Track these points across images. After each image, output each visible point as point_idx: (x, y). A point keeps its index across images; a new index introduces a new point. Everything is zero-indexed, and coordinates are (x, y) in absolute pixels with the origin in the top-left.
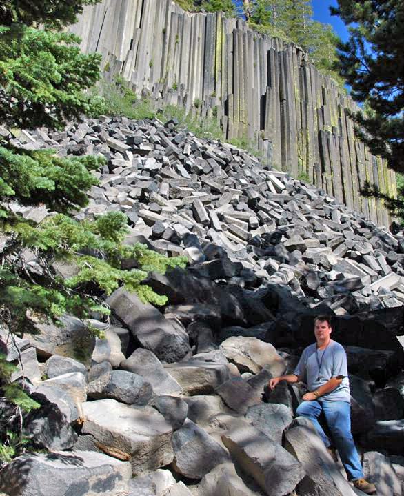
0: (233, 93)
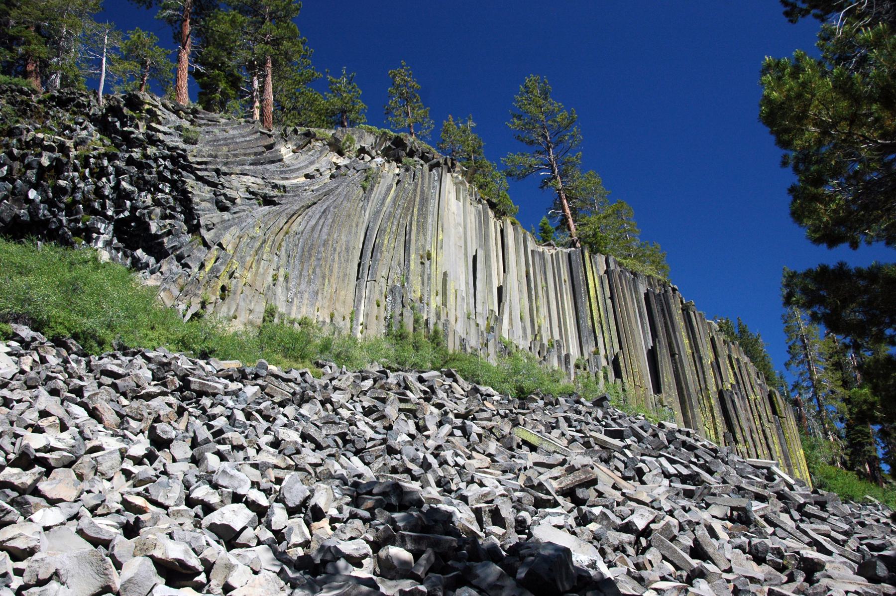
0: (621, 348)
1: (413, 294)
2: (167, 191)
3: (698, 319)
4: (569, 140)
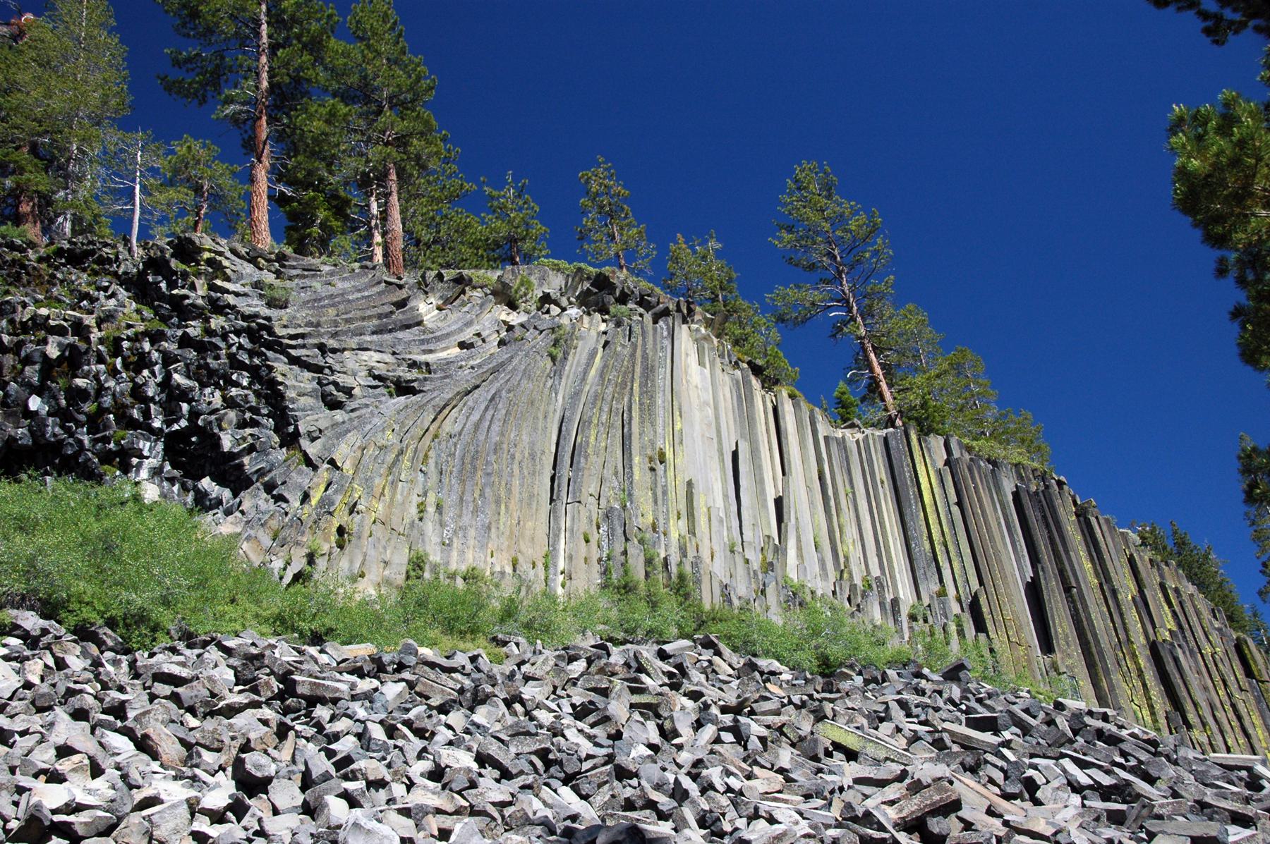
0: (981, 583)
1: (640, 519)
2: (245, 383)
3: (1105, 528)
4: (872, 257)
